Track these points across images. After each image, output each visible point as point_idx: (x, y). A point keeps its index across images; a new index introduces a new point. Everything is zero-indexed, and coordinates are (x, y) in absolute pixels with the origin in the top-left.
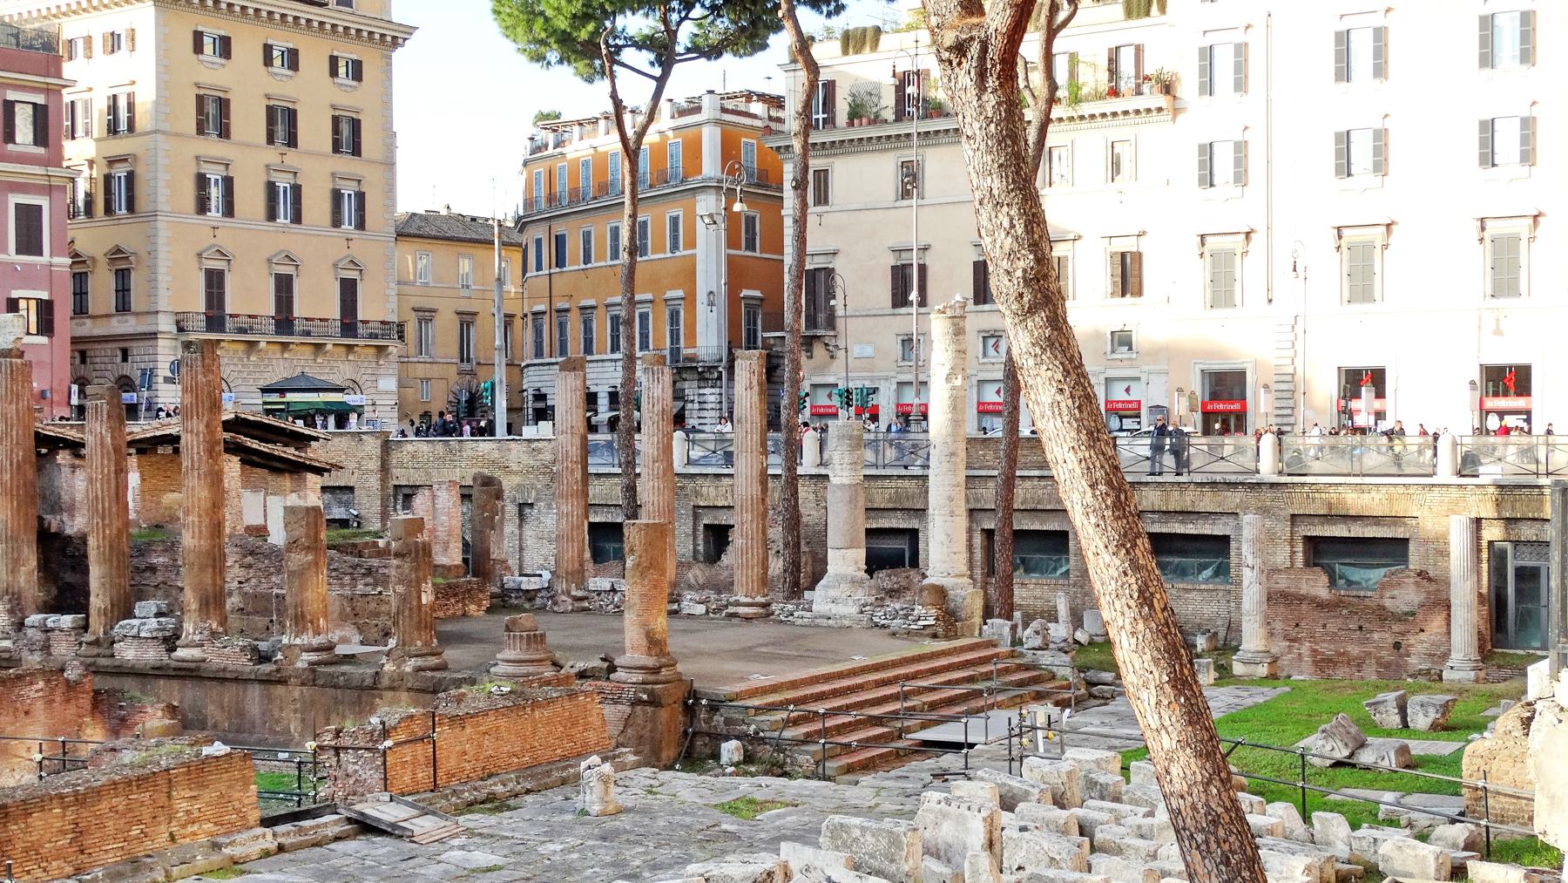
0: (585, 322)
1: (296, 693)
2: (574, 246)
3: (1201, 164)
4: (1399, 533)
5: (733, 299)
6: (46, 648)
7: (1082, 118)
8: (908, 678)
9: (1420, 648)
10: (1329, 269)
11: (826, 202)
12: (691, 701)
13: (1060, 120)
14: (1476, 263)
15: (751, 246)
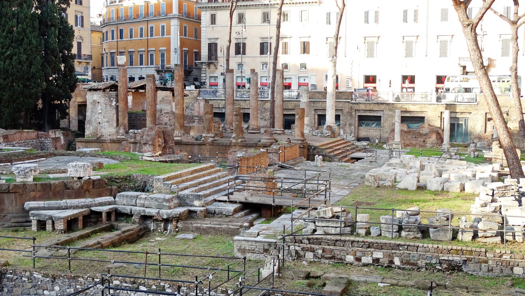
0: (130, 56)
1: (208, 147)
2: (126, 32)
3: (327, 18)
4: (423, 115)
5: (182, 51)
6: (135, 138)
7: (293, 3)
8: (336, 146)
9: (429, 142)
10: (364, 48)
11: (215, 24)
12: (309, 147)
13: (287, 4)
14: (402, 47)
15: (185, 35)
